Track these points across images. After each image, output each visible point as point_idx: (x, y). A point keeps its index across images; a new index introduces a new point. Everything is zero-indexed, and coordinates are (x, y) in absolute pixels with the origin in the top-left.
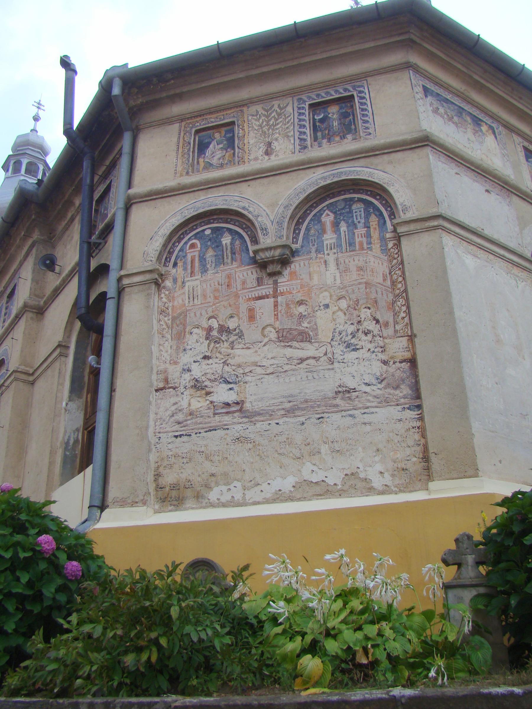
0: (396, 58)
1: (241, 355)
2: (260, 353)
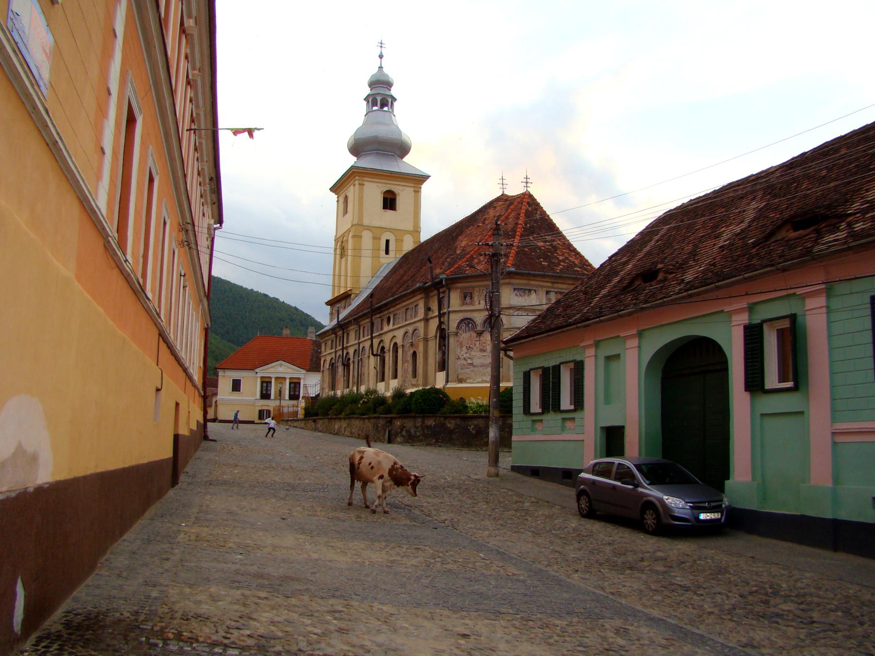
0: (507, 281)
1: (473, 353)
2: (476, 353)
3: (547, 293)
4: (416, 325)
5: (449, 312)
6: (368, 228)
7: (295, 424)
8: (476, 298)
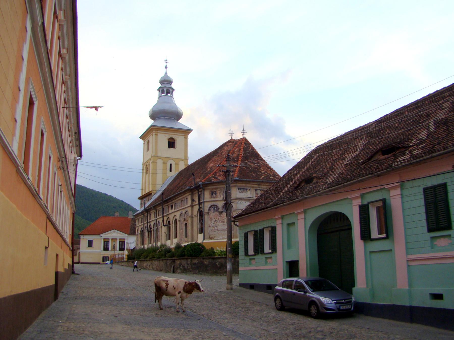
0: (235, 184)
1: (217, 224)
2: (219, 223)
3: (256, 190)
4: (187, 209)
5: (204, 202)
6: (161, 158)
7: (123, 264)
8: (218, 194)
